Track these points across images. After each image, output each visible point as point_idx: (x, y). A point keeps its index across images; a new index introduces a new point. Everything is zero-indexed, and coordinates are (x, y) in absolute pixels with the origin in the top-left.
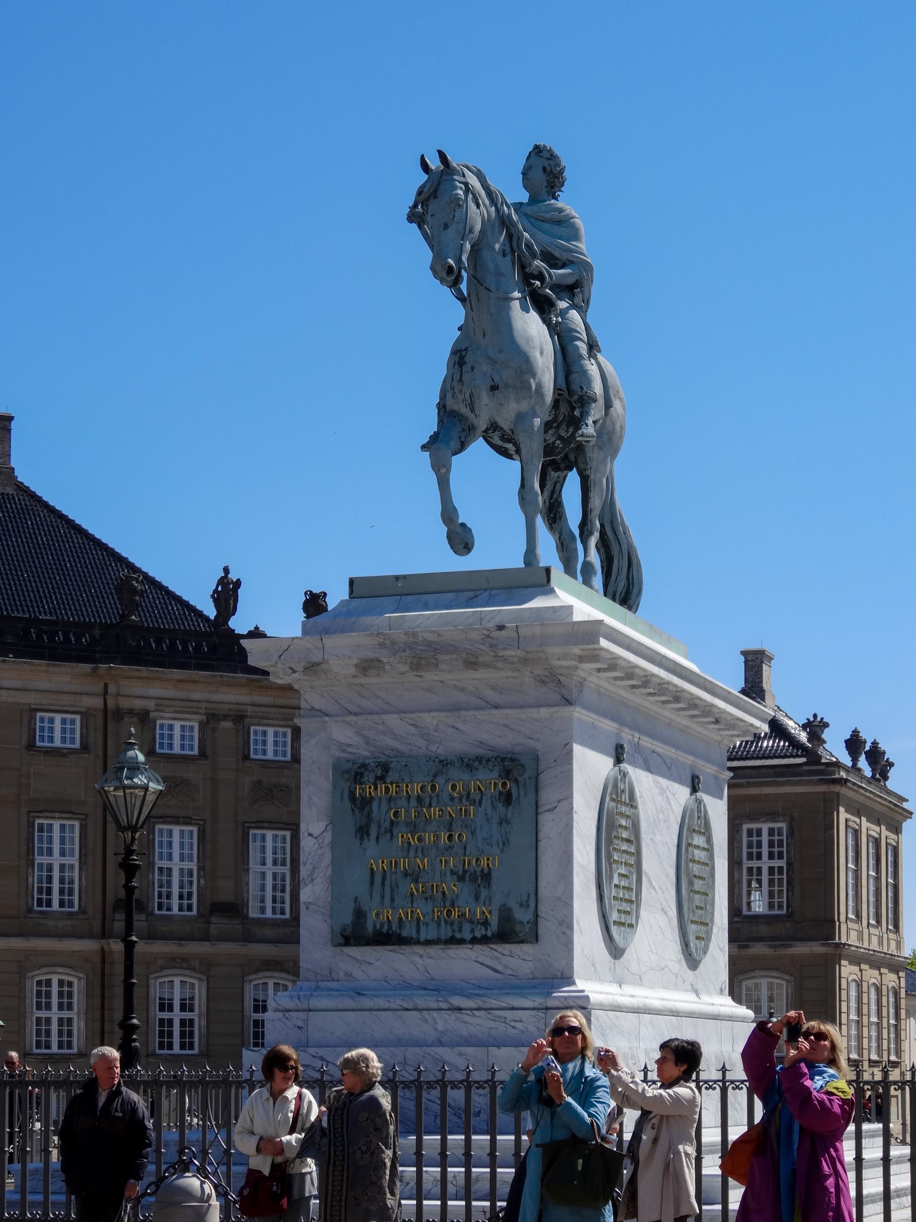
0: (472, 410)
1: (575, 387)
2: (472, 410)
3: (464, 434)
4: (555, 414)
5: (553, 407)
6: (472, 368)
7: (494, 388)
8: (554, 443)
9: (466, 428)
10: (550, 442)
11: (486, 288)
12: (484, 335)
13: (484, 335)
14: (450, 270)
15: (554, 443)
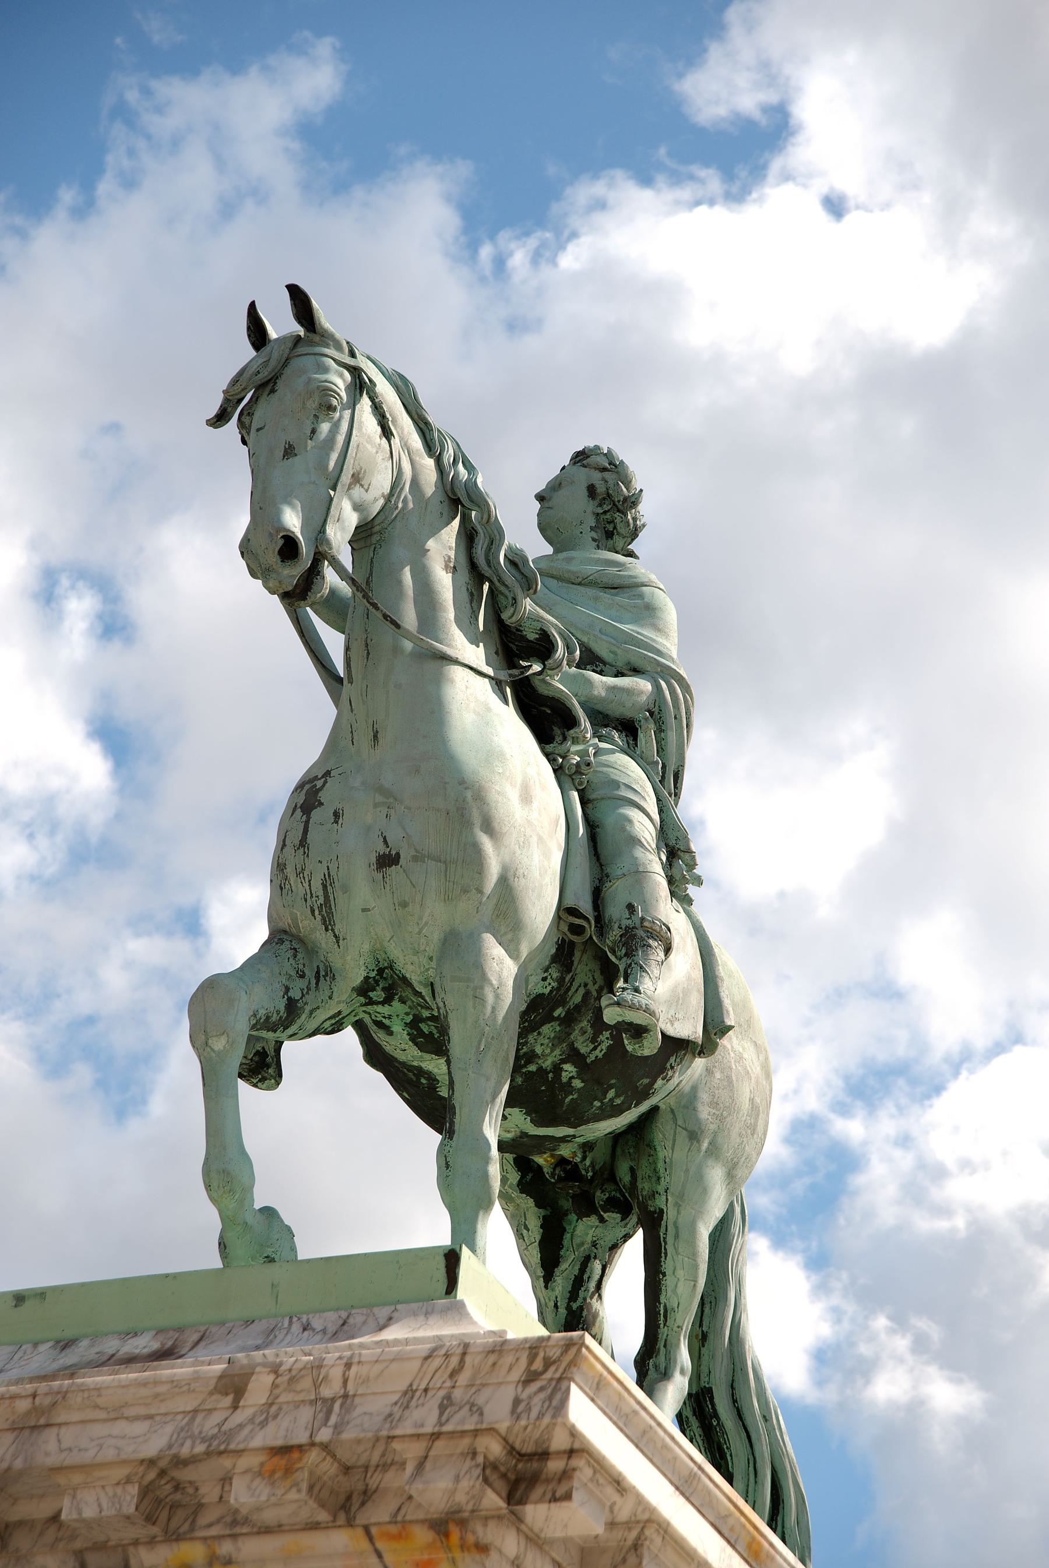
0: (328, 924)
1: (615, 911)
2: (328, 924)
3: (302, 984)
4: (561, 981)
5: (555, 959)
6: (336, 815)
7: (387, 861)
8: (557, 1069)
9: (310, 973)
10: (547, 1064)
11: (385, 617)
12: (375, 737)
13: (375, 737)
14: (289, 548)
15: (557, 1069)
